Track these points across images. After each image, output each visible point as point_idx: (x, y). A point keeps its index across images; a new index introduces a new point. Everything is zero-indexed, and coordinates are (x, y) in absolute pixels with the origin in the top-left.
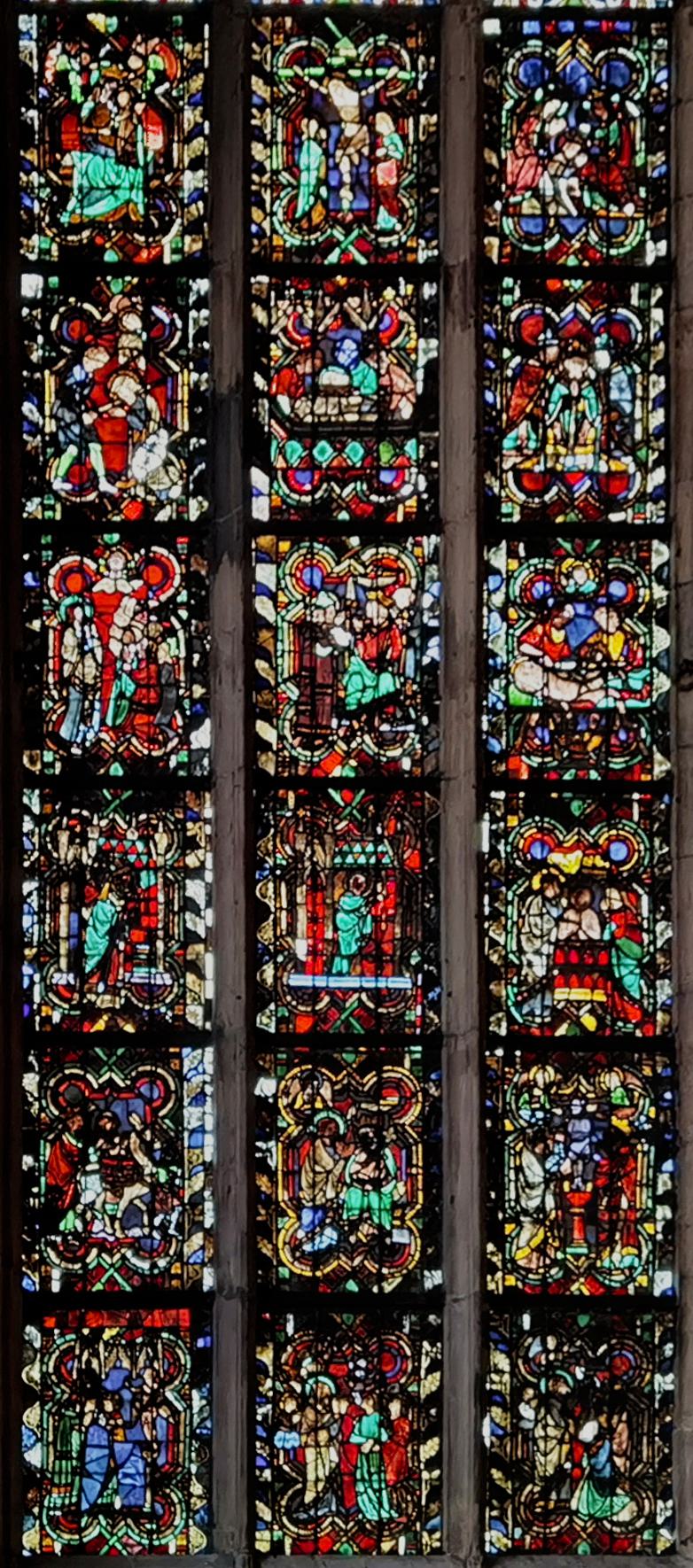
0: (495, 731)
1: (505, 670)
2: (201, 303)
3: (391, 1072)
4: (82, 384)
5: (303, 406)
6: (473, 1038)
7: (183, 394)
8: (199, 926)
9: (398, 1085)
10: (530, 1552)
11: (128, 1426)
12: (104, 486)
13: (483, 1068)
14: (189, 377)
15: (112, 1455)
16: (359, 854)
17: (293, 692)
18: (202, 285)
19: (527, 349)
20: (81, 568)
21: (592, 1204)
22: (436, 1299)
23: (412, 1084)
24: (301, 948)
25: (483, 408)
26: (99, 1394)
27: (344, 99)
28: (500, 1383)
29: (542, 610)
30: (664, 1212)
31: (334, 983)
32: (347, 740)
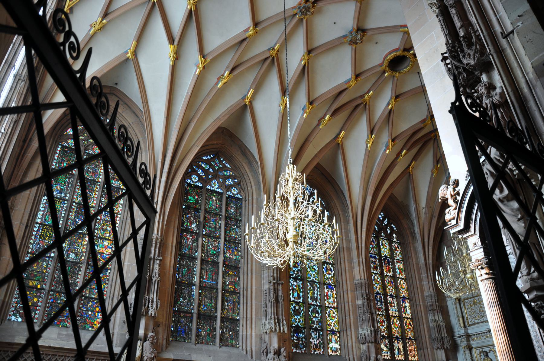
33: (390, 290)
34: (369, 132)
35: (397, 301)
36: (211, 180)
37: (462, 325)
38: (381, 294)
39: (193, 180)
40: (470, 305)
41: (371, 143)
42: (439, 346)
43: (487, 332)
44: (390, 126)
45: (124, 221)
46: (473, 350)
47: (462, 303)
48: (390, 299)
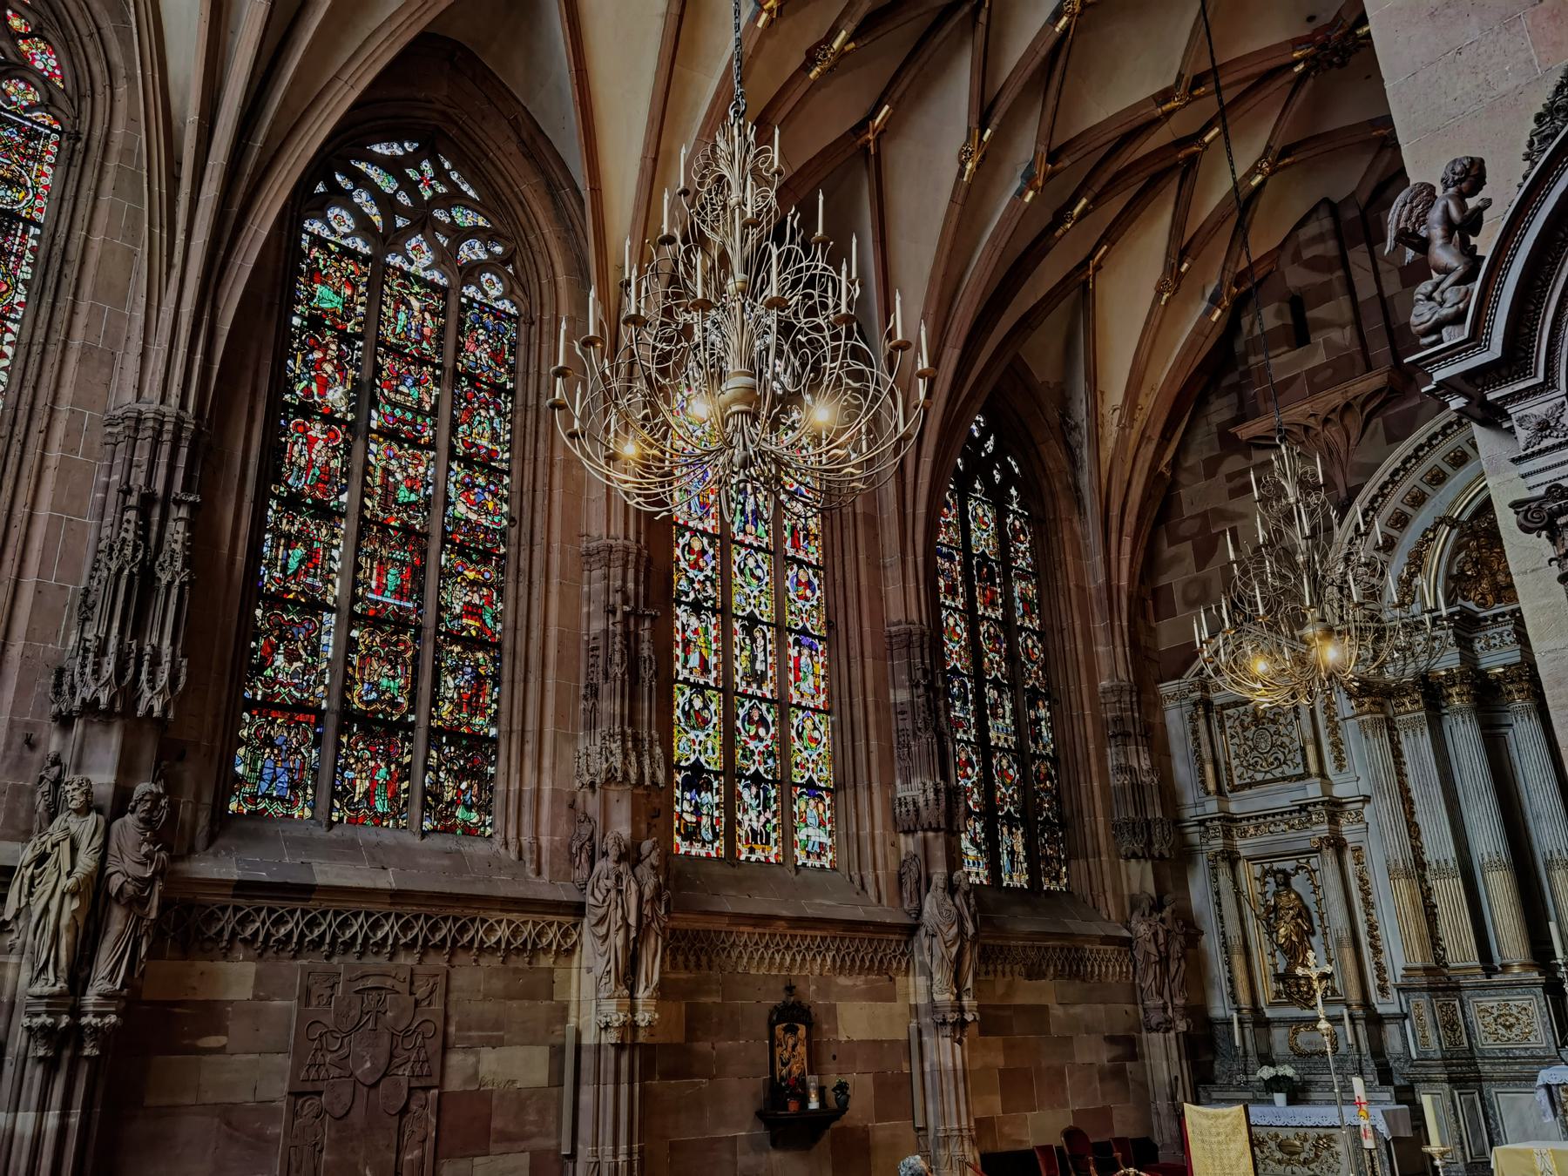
0: (449, 524)
1: (454, 504)
2: (359, 349)
3: (402, 637)
4: (312, 361)
5: (392, 395)
6: (433, 631)
7: (350, 377)
8: (336, 567)
9: (405, 642)
10: (439, 832)
11: (283, 761)
12: (316, 398)
13: (436, 642)
14: (352, 372)
15: (275, 772)
16: (398, 555)
17: (380, 492)
18: (360, 344)
19: (469, 402)
20: (304, 424)
21: (470, 699)
22: (412, 726)
23: (410, 643)
24: (374, 584)
25: (453, 416)
26: (272, 746)
27: (415, 304)
28: (433, 762)
29: (468, 487)
30: (494, 706)
31: (384, 600)
32: (398, 513)
33: (995, 665)
34: (976, 117)
35: (1011, 700)
36: (406, 233)
37: (1212, 787)
38: (964, 675)
39: (334, 224)
40: (1242, 725)
41: (977, 158)
42: (1137, 847)
43: (1291, 812)
44: (1051, 102)
45: (36, 349)
46: (1242, 865)
47: (1215, 717)
48: (993, 694)
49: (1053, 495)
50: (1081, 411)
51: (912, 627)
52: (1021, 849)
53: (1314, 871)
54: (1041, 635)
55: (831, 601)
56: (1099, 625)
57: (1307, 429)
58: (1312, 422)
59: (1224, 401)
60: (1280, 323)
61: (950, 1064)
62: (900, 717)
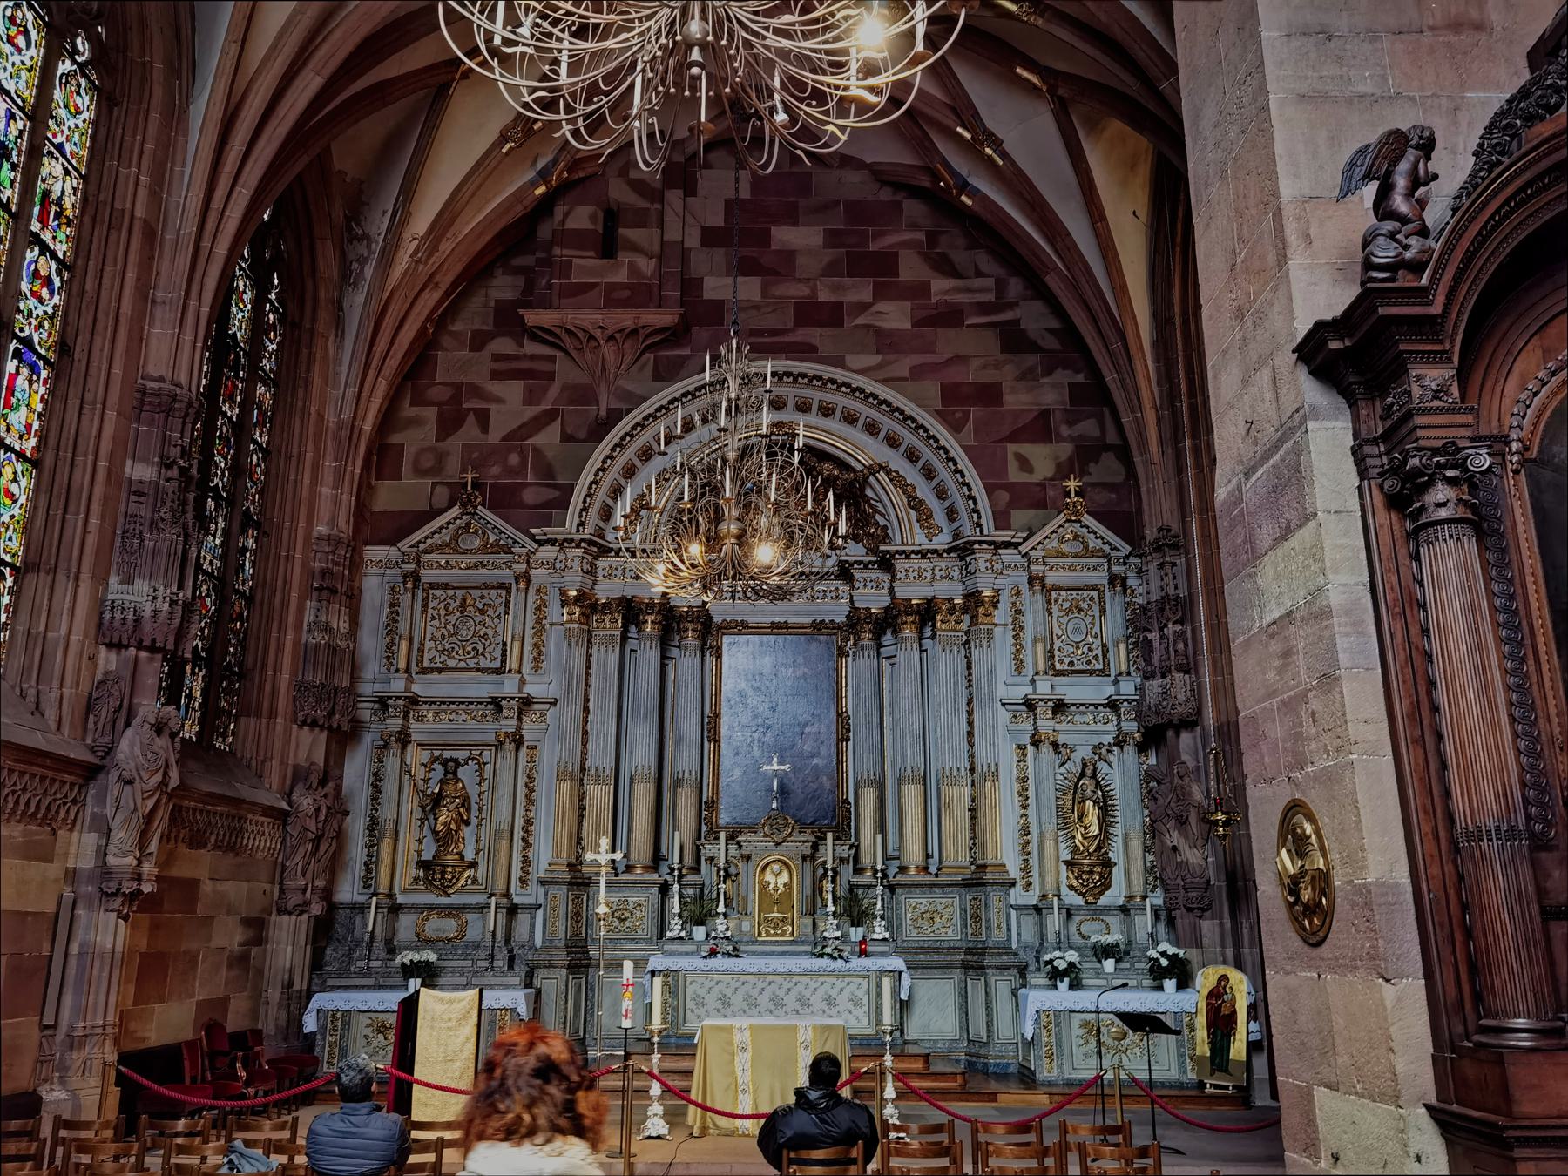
40: (446, 608)
42: (320, 714)
46: (410, 749)
49: (316, 300)
50: (378, 225)
51: (178, 391)
52: (198, 694)
53: (485, 764)
54: (266, 452)
55: (73, 317)
56: (328, 464)
57: (591, 337)
58: (598, 334)
59: (509, 279)
60: (591, 227)
61: (109, 946)
62: (133, 498)
